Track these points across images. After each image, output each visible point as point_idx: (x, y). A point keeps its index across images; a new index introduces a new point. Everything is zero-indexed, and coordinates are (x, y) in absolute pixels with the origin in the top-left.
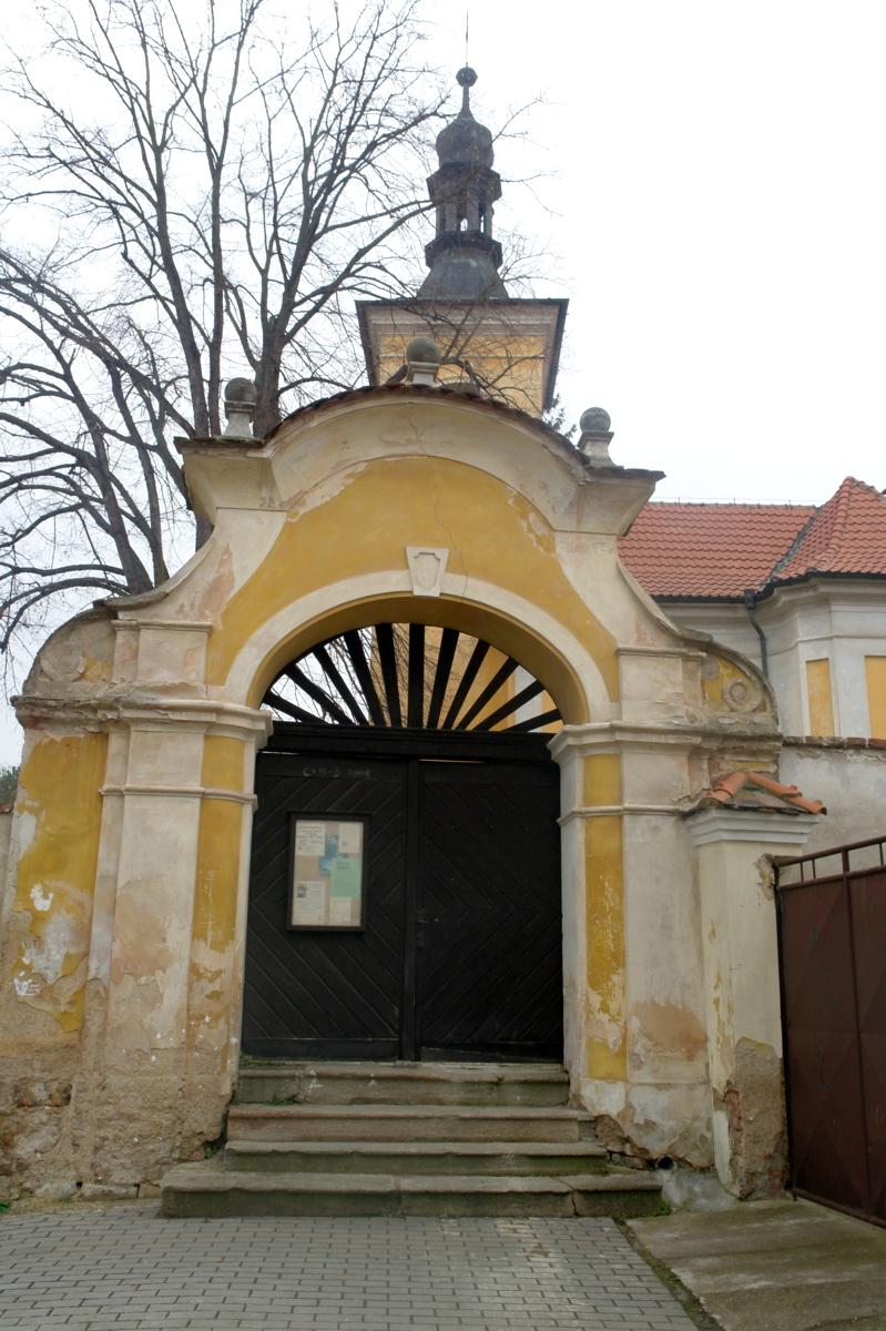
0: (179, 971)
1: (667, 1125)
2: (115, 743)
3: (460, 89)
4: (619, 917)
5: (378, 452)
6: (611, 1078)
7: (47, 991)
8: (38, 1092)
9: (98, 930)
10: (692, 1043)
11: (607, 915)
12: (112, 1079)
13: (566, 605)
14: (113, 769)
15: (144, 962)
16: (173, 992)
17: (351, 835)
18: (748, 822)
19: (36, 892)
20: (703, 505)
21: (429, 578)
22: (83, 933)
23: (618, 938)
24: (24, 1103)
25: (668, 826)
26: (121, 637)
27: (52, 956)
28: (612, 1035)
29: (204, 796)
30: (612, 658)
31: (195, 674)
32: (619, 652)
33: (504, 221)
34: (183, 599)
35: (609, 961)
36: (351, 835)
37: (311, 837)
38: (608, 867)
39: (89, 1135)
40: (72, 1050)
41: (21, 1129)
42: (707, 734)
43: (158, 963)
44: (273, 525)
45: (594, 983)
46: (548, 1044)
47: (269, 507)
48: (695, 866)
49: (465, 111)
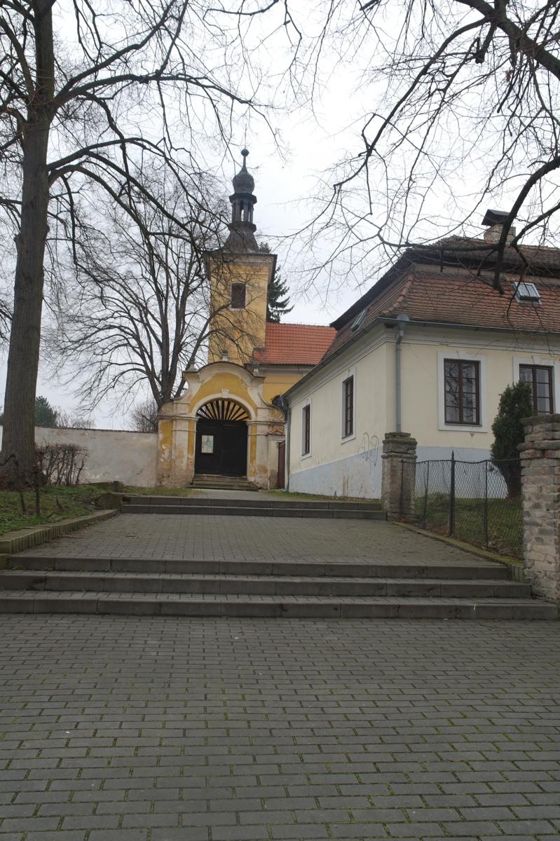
0: (186, 458)
2: (174, 422)
3: (242, 157)
4: (255, 451)
5: (217, 372)
7: (165, 461)
9: (173, 452)
10: (266, 471)
11: (254, 451)
14: (174, 427)
15: (181, 457)
16: (185, 460)
17: (211, 438)
18: (274, 437)
19: (163, 446)
20: (323, 327)
21: (225, 394)
22: (171, 452)
23: (255, 454)
24: (163, 477)
25: (264, 437)
26: (175, 405)
27: (166, 455)
28: (253, 470)
29: (189, 431)
30: (256, 409)
31: (187, 411)
33: (261, 216)
35: (254, 458)
36: (211, 438)
37: (205, 438)
38: (254, 443)
39: (173, 481)
40: (170, 470)
43: (182, 457)
44: (199, 385)
45: (251, 462)
46: (245, 473)
47: (199, 382)
48: (268, 444)
49: (244, 169)
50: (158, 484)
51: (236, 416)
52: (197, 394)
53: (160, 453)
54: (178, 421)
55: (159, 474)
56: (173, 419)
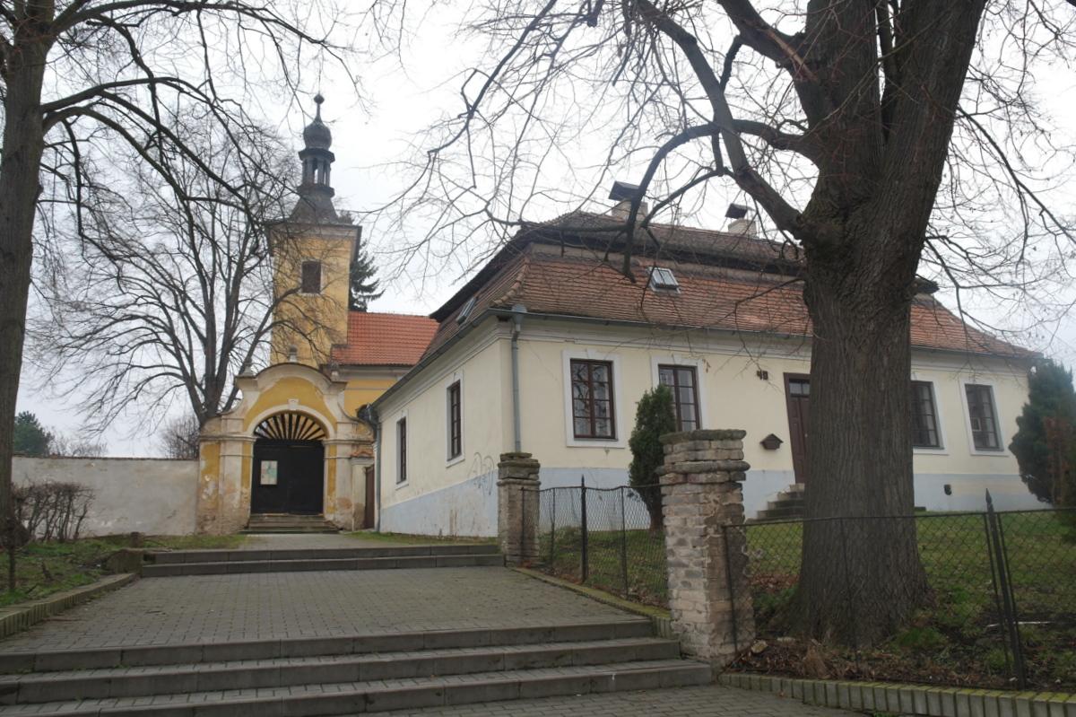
0: (238, 493)
1: (342, 522)
2: (222, 445)
4: (334, 480)
5: (282, 376)
6: (331, 513)
7: (209, 497)
8: (209, 517)
9: (220, 485)
10: (349, 506)
11: (332, 480)
12: (226, 515)
13: (325, 412)
14: (222, 450)
15: (231, 491)
16: (237, 496)
17: (274, 464)
18: (360, 460)
19: (206, 477)
21: (294, 406)
22: (217, 485)
23: (334, 484)
24: (206, 520)
25: (346, 461)
27: (210, 490)
28: (332, 505)
29: (243, 456)
30: (335, 424)
31: (240, 429)
32: (337, 423)
33: (338, 177)
34: (237, 412)
35: (332, 489)
36: (274, 464)
37: (265, 465)
38: (333, 470)
39: (220, 525)
40: (215, 509)
41: (206, 525)
42: (355, 441)
43: (234, 491)
46: (320, 509)
47: (256, 390)
48: (352, 471)
49: (318, 119)
50: (199, 530)
51: (309, 433)
52: (254, 406)
53: (201, 487)
54: (227, 444)
55: (199, 517)
56: (220, 440)
